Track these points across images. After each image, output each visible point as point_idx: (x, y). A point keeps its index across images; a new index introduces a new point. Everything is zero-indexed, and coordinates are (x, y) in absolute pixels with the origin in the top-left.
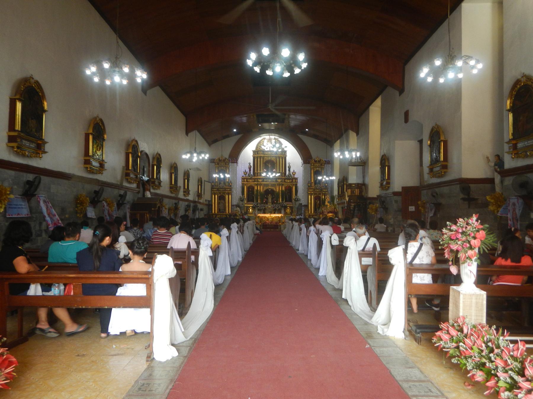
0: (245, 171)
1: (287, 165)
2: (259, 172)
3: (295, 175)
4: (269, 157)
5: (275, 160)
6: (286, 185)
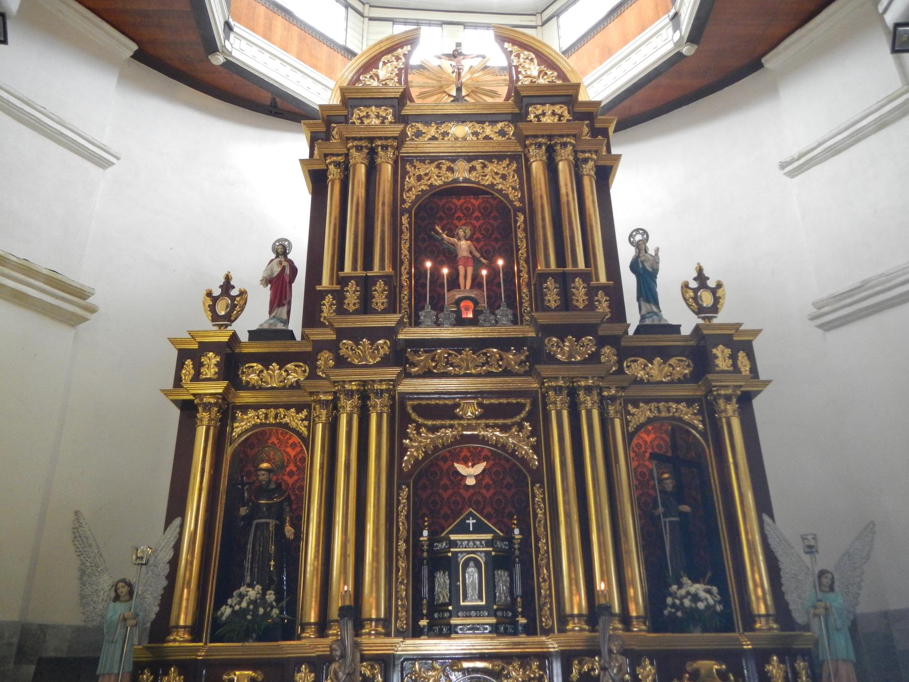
0: (227, 286)
1: (626, 253)
2: (360, 272)
3: (714, 309)
4: (453, 160)
5: (513, 180)
6: (641, 414)
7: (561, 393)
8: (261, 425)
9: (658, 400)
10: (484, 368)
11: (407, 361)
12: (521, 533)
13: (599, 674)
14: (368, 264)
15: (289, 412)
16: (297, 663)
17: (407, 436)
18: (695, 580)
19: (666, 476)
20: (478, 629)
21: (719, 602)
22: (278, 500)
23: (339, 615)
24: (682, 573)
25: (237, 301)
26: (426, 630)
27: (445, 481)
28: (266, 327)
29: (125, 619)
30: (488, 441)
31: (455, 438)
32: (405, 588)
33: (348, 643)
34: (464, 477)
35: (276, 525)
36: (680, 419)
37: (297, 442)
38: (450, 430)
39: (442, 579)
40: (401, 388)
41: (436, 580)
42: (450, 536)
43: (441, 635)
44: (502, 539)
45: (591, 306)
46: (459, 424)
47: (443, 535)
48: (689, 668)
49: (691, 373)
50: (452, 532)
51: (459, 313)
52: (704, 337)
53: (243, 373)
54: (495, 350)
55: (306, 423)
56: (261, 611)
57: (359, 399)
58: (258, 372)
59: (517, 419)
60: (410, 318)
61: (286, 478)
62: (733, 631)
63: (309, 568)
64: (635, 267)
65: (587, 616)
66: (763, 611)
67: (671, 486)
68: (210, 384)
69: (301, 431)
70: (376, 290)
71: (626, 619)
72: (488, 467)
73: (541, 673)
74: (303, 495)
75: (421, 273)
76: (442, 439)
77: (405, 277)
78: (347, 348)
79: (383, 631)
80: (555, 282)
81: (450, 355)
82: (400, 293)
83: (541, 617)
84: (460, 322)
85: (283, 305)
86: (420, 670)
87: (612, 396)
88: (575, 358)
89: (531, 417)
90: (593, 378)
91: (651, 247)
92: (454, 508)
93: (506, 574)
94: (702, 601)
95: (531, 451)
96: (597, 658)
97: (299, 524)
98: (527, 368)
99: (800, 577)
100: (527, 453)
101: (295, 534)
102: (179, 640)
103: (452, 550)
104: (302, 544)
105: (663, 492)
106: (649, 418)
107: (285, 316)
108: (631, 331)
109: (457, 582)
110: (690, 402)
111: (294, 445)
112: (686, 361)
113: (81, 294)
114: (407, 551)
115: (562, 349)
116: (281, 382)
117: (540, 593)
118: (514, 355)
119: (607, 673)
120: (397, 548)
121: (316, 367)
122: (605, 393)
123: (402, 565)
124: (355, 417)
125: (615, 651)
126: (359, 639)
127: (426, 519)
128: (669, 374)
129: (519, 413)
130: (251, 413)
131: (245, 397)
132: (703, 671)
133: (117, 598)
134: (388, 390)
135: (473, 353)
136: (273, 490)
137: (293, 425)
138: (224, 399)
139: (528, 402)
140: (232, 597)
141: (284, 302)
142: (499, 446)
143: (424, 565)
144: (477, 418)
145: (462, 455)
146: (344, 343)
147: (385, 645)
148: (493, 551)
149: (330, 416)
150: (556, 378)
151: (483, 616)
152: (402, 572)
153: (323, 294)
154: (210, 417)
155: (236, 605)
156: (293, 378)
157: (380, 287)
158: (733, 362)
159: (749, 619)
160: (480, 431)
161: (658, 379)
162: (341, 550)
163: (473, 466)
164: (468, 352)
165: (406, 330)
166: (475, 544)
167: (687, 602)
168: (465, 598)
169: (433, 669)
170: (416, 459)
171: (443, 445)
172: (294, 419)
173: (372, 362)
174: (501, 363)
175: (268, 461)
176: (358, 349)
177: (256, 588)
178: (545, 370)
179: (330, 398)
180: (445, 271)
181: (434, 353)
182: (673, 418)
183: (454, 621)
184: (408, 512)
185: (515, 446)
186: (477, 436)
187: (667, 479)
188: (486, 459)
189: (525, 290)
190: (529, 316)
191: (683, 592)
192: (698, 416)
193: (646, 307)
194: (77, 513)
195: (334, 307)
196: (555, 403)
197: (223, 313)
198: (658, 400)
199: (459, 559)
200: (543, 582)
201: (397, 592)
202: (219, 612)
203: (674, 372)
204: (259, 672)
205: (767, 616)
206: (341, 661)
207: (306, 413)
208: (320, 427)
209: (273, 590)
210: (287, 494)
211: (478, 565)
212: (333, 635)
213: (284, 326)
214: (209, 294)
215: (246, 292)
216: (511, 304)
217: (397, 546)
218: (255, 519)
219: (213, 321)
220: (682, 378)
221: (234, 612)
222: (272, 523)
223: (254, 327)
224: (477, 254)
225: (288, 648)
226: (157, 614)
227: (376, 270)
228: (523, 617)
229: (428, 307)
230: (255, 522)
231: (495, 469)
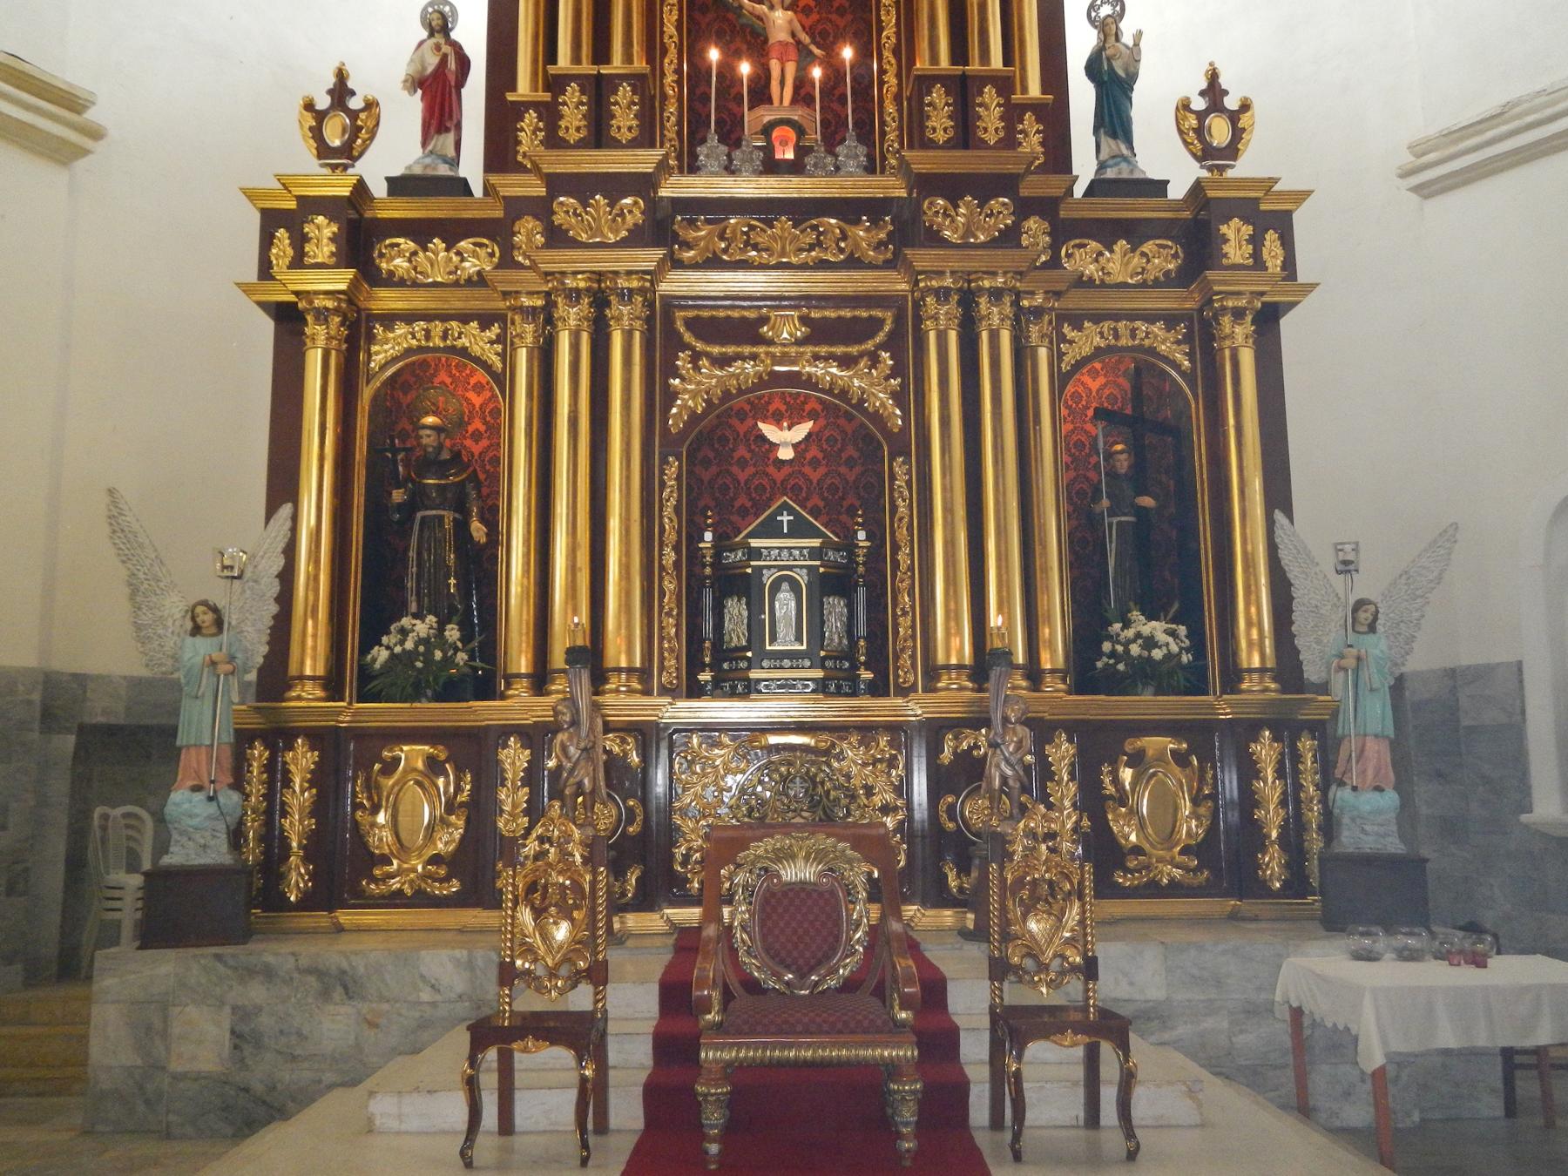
0: (341, 91)
1: (1080, 42)
2: (586, 68)
3: (1232, 151)
6: (1085, 340)
7: (947, 300)
8: (420, 349)
9: (1116, 316)
10: (813, 253)
11: (675, 237)
12: (867, 539)
13: (986, 754)
14: (601, 53)
15: (467, 327)
16: (506, 731)
17: (676, 375)
18: (1151, 617)
19: (1119, 447)
20: (794, 686)
21: (1188, 650)
22: (457, 480)
23: (567, 662)
24: (1132, 604)
25: (362, 121)
26: (709, 687)
27: (742, 451)
28: (418, 171)
29: (213, 663)
30: (817, 383)
31: (760, 377)
32: (674, 622)
33: (583, 704)
34: (775, 447)
35: (454, 519)
36: (1152, 351)
37: (484, 382)
38: (752, 363)
39: (736, 610)
40: (664, 288)
41: (726, 611)
42: (750, 540)
43: (733, 695)
44: (837, 548)
45: (1009, 141)
46: (767, 354)
47: (737, 539)
48: (1128, 748)
49: (1179, 269)
50: (752, 535)
51: (768, 150)
52: (1207, 203)
53: (382, 255)
54: (833, 221)
55: (499, 348)
56: (438, 655)
57: (591, 305)
58: (407, 255)
59: (869, 345)
60: (679, 158)
61: (468, 443)
62: (1207, 694)
63: (515, 589)
64: (1094, 68)
65: (971, 667)
66: (1256, 663)
67: (1126, 464)
68: (324, 274)
69: (490, 362)
70: (616, 103)
71: (1034, 674)
72: (817, 429)
73: (894, 752)
74: (499, 425)
75: (699, 73)
76: (738, 379)
77: (670, 78)
78: (567, 212)
79: (639, 687)
80: (947, 94)
81: (752, 228)
82: (662, 110)
83: (897, 668)
84: (771, 167)
85: (447, 130)
86: (700, 746)
87: (1036, 307)
88: (976, 237)
89: (894, 344)
90: (1005, 273)
91: (1127, 28)
92: (757, 449)
93: (842, 603)
94: (1160, 647)
95: (890, 402)
96: (983, 731)
97: (491, 519)
98: (889, 255)
99: (1321, 611)
100: (883, 404)
101: (487, 535)
102: (307, 698)
103: (752, 563)
104: (502, 552)
105: (1112, 475)
106: (1098, 349)
107: (451, 152)
108: (1079, 190)
109: (760, 614)
110: (1171, 320)
111: (479, 388)
112: (1171, 248)
113: (71, 102)
114: (677, 564)
115: (953, 221)
116: (450, 273)
117: (896, 632)
118: (867, 230)
119: (998, 751)
120: (660, 560)
121: (513, 247)
122: (1025, 303)
123: (669, 585)
124: (585, 337)
125: (1013, 720)
126: (600, 699)
127: (710, 513)
128: (1140, 270)
129: (872, 336)
130: (401, 329)
131: (387, 300)
132: (1150, 752)
133: (197, 630)
134: (641, 291)
135: (794, 227)
136: (446, 461)
137: (476, 350)
138: (350, 302)
139: (888, 316)
140: (388, 633)
141: (448, 125)
142: (836, 392)
143: (706, 587)
144: (799, 342)
145: (772, 408)
146: (562, 203)
147: (644, 707)
148: (821, 566)
149: (540, 336)
150: (940, 274)
151: (803, 668)
152: (670, 598)
153: (520, 109)
154: (327, 333)
155: (395, 645)
156: (471, 267)
157: (624, 97)
158: (1254, 249)
159: (1232, 676)
160: (804, 367)
161: (1120, 279)
162: (567, 559)
163: (790, 428)
164: (784, 224)
165: (672, 179)
166: (791, 555)
167: (1135, 649)
168: (773, 639)
169: (718, 744)
170: (693, 414)
171: (739, 389)
172: (478, 341)
173: (612, 238)
174: (843, 245)
175: (435, 414)
176: (587, 213)
177: (427, 620)
178: (922, 258)
179: (540, 303)
180: (745, 68)
181: (722, 225)
182: (1140, 349)
183: (754, 674)
184: (679, 501)
185: (863, 393)
186: (798, 373)
187: (1121, 452)
188: (813, 415)
189: (890, 108)
190: (897, 159)
191: (1130, 633)
192: (1182, 347)
193: (1110, 147)
194: (111, 492)
195: (541, 135)
196: (935, 318)
197: (337, 143)
198: (1116, 316)
199: (764, 579)
200: (901, 616)
201: (661, 628)
202: (369, 657)
203: (1149, 267)
204: (441, 747)
205: (1262, 670)
206: (571, 730)
207: (499, 331)
208: (522, 355)
209: (457, 624)
210: (471, 469)
211: (795, 587)
212: (558, 692)
213: (451, 170)
214: (309, 106)
215: (378, 104)
216: (865, 132)
217: (661, 555)
218: (419, 510)
219: (319, 157)
220: (1162, 279)
221: (393, 656)
222: (449, 516)
223: (397, 171)
224: (806, 39)
225: (485, 712)
226: (265, 657)
227: (617, 65)
228: (866, 670)
229: (713, 139)
230: (419, 515)
231: (827, 433)
